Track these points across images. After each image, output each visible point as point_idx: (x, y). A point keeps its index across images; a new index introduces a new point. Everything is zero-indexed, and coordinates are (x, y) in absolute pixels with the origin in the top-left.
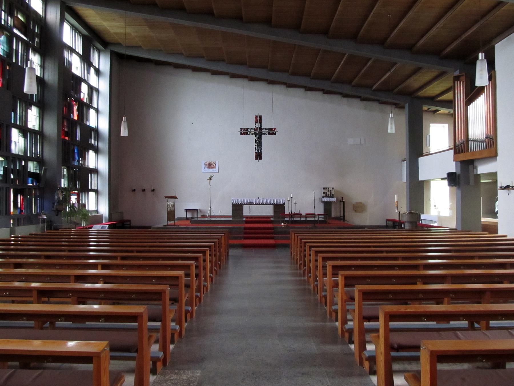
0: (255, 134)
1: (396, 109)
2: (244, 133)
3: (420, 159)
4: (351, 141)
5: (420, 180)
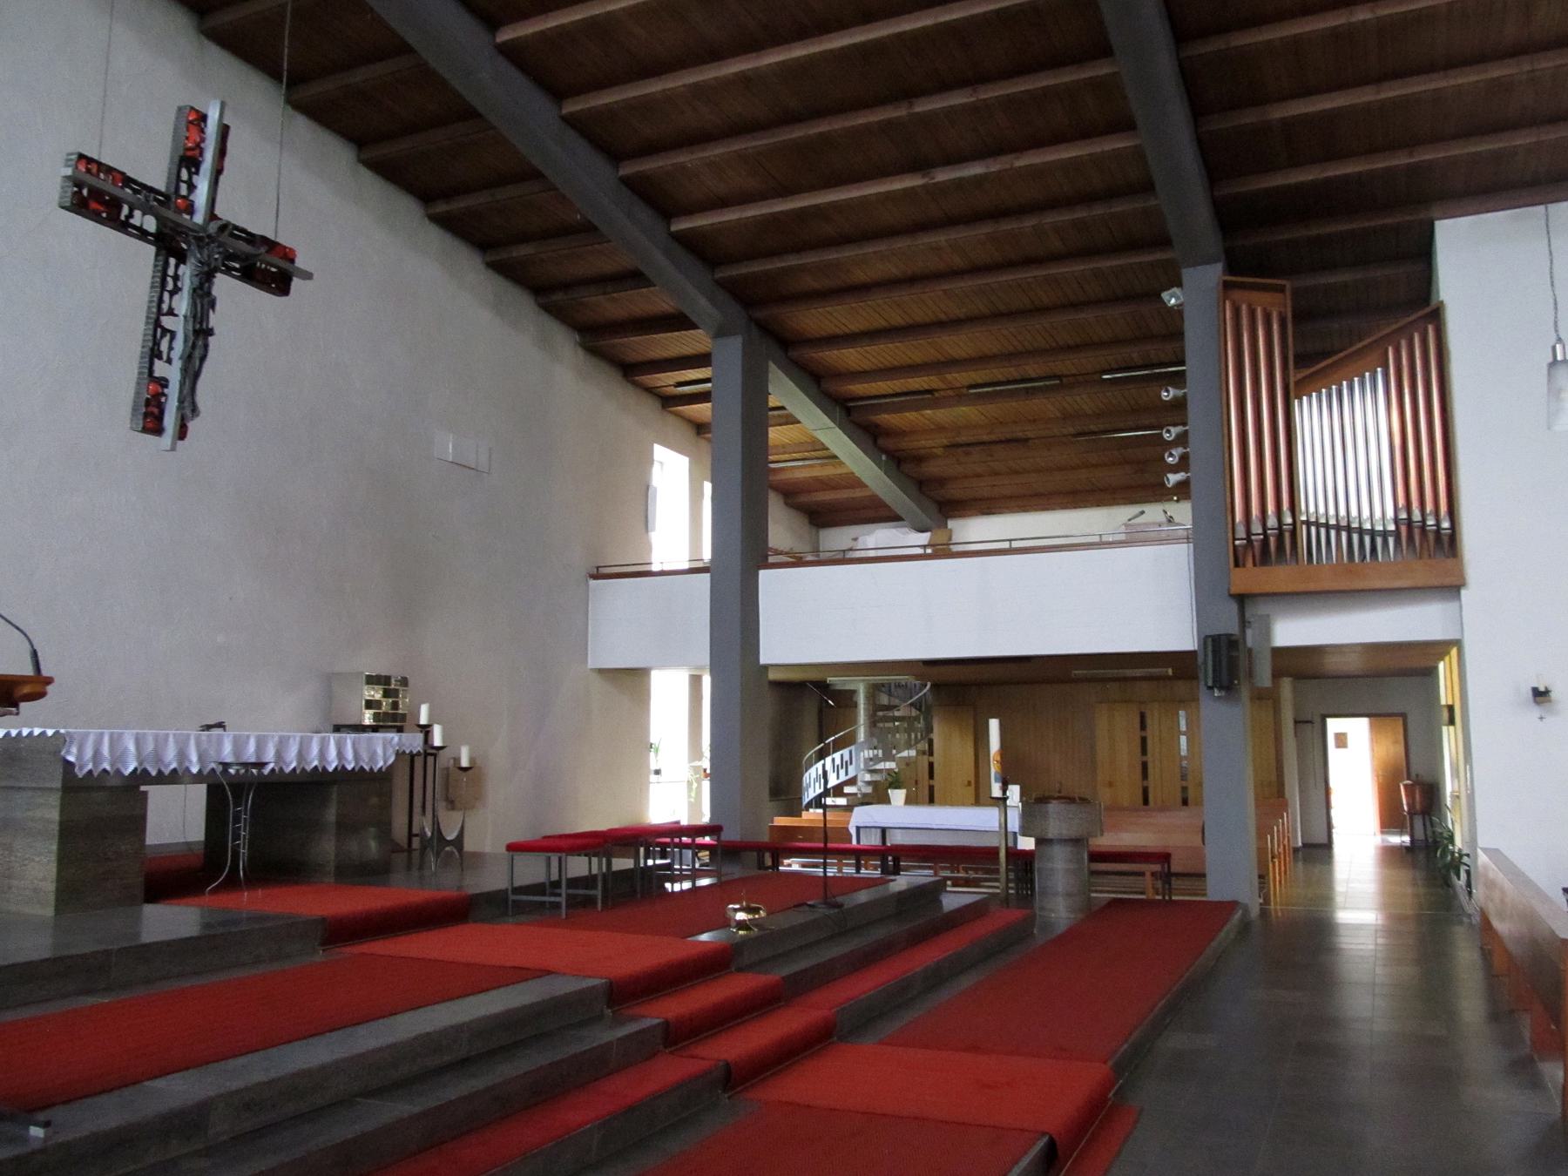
0: (169, 243)
1: (581, 352)
2: (96, 194)
3: (762, 573)
4: (447, 446)
5: (762, 661)
